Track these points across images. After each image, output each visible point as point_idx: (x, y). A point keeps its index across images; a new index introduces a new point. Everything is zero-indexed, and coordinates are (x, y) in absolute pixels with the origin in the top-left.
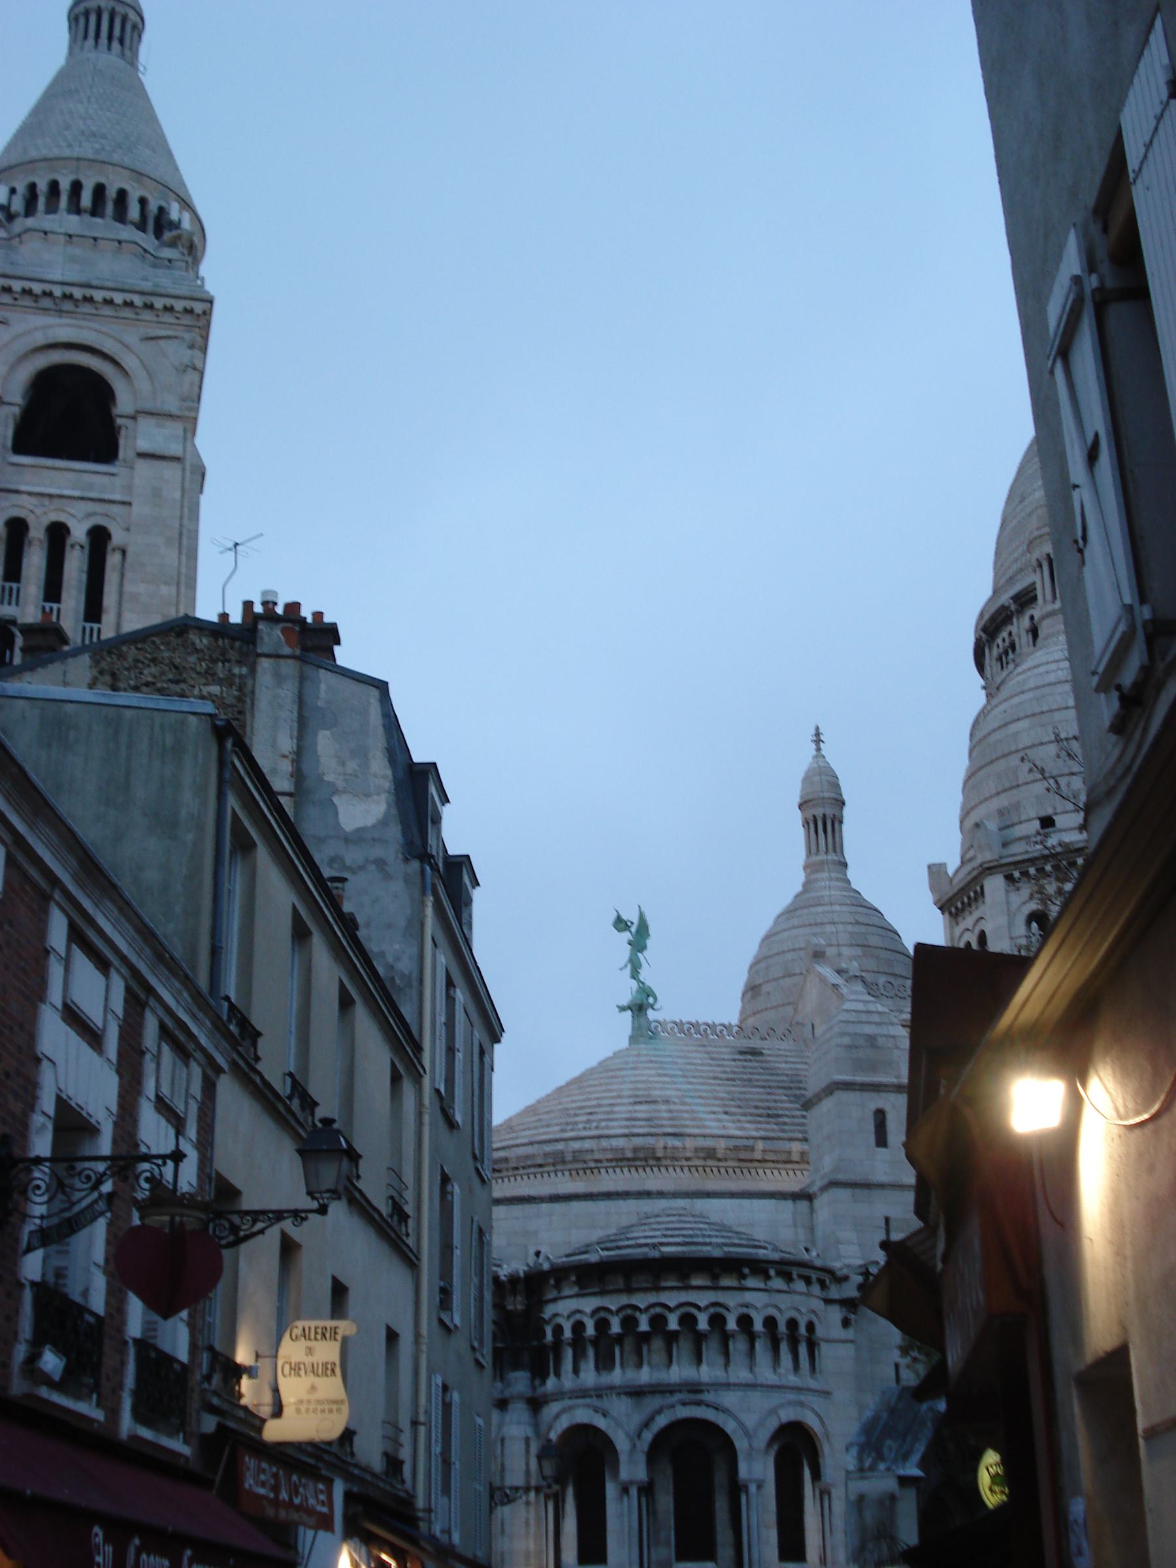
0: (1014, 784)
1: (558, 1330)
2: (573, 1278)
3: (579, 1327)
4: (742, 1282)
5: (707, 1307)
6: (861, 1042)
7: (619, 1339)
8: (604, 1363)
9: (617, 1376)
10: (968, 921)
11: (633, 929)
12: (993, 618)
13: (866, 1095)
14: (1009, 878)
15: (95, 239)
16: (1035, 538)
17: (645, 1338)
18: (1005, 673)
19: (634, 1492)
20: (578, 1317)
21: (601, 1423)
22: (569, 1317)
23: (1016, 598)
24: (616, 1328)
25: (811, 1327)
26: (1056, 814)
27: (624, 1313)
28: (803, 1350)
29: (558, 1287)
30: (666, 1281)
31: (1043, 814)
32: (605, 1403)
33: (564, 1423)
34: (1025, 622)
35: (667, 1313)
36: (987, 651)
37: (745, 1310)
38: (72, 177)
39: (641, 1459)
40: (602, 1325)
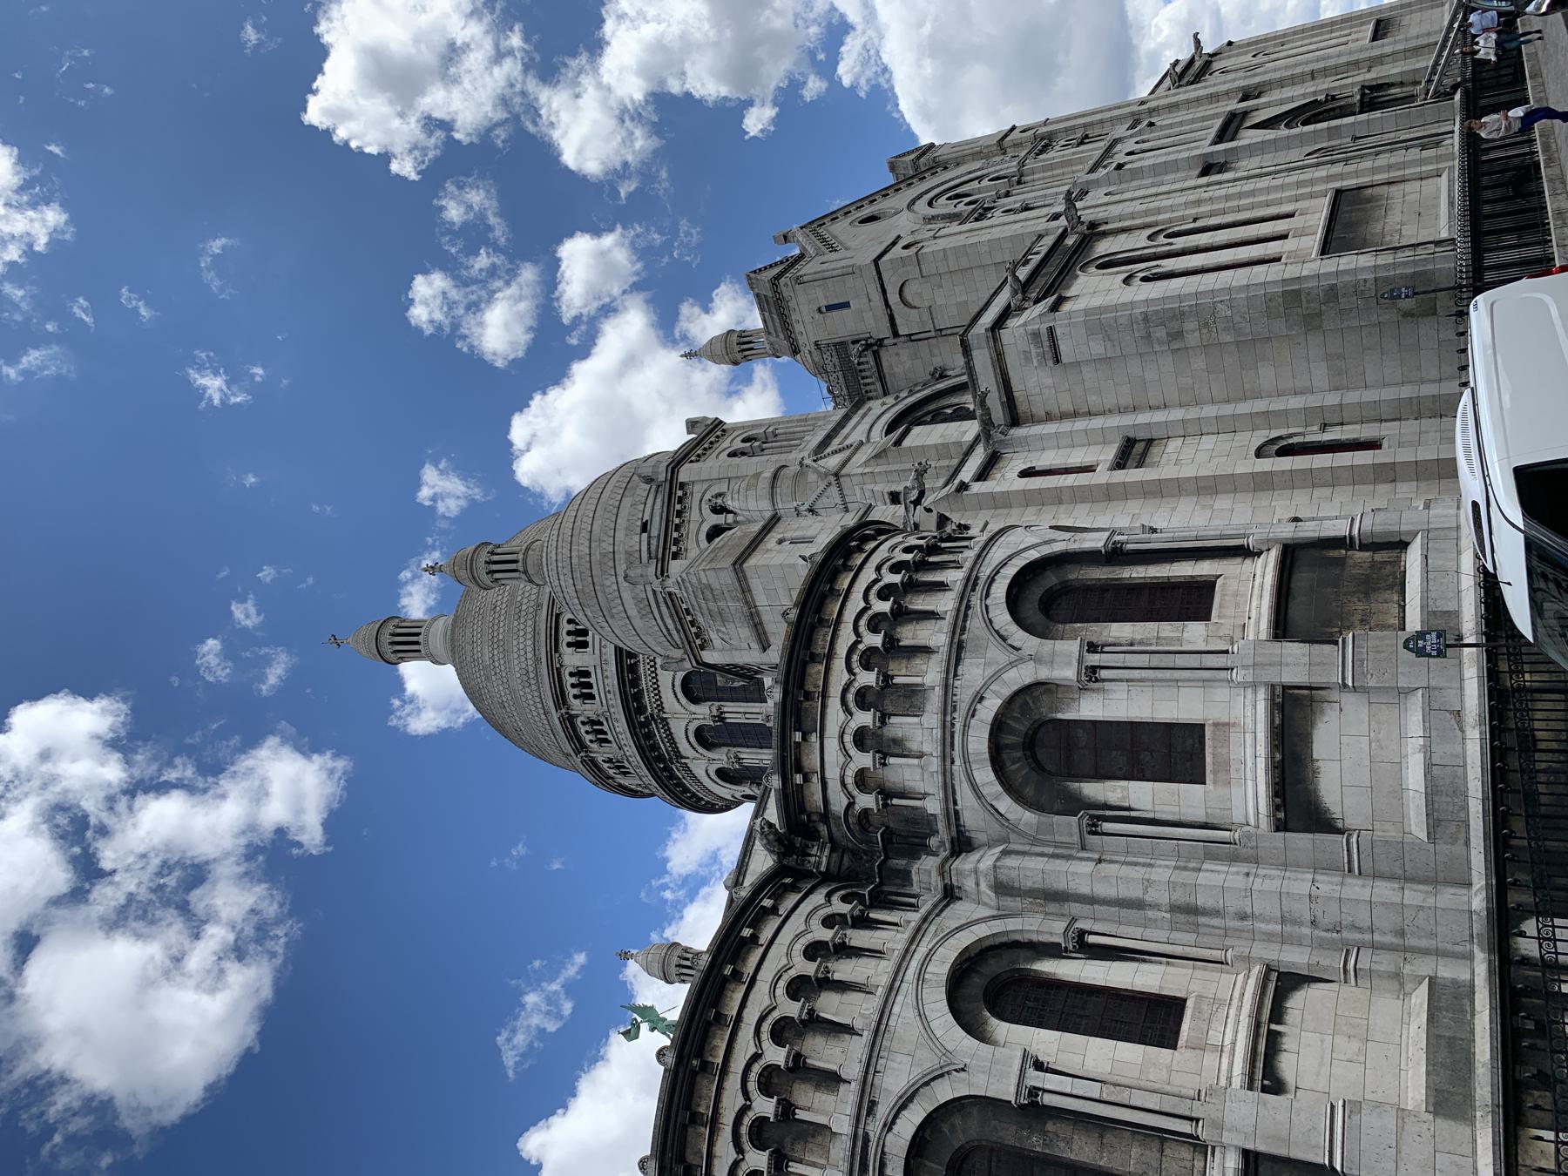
1: (862, 779)
2: (798, 736)
3: (861, 739)
6: (712, 555)
8: (912, 698)
11: (639, 1019)
12: (570, 739)
13: (762, 546)
14: (675, 556)
16: (472, 573)
17: (892, 645)
18: (610, 737)
19: (1094, 659)
20: (848, 739)
21: (990, 707)
23: (558, 707)
24: (868, 678)
30: (831, 615)
31: (638, 530)
32: (964, 697)
33: (985, 776)
34: (576, 703)
35: (870, 612)
36: (592, 755)
39: (1048, 644)
40: (864, 699)
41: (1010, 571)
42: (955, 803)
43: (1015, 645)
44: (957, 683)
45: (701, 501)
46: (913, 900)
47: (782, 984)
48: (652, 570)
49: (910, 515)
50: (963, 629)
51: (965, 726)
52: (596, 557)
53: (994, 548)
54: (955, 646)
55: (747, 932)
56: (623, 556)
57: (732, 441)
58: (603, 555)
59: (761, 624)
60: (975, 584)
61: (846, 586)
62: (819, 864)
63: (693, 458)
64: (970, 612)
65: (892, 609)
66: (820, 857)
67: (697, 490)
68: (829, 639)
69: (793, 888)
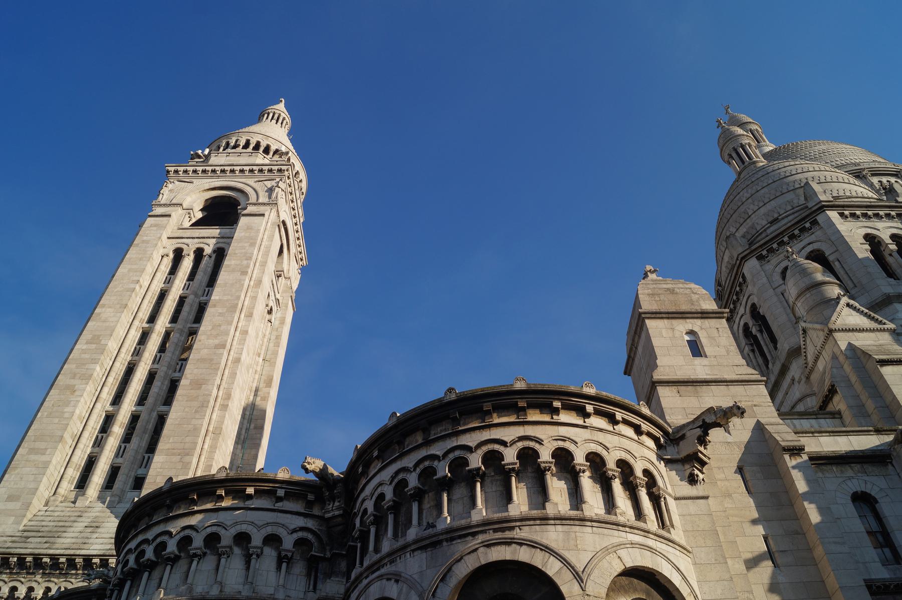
0: (747, 216)
2: (376, 453)
4: (555, 417)
5: (513, 442)
6: (660, 292)
7: (419, 495)
9: (412, 533)
10: (741, 311)
13: (675, 322)
14: (760, 258)
15: (241, 153)
22: (372, 495)
25: (646, 472)
26: (780, 215)
27: (422, 466)
28: (643, 494)
29: (365, 473)
30: (465, 424)
31: (771, 219)
37: (561, 444)
38: (237, 138)
41: (524, 555)
42: (353, 591)
43: (438, 591)
44: (408, 555)
45: (809, 244)
46: (311, 587)
47: (214, 529)
48: (740, 250)
49: (691, 427)
50: (452, 539)
51: (382, 576)
52: (742, 209)
53: (559, 528)
54: (434, 539)
55: (250, 490)
56: (750, 224)
57: (891, 227)
58: (745, 212)
59: (633, 360)
60: (503, 530)
61: (497, 420)
62: (329, 512)
63: (847, 213)
64: (470, 538)
65: (470, 471)
66: (332, 510)
67: (818, 234)
68: (443, 434)
69: (309, 504)
